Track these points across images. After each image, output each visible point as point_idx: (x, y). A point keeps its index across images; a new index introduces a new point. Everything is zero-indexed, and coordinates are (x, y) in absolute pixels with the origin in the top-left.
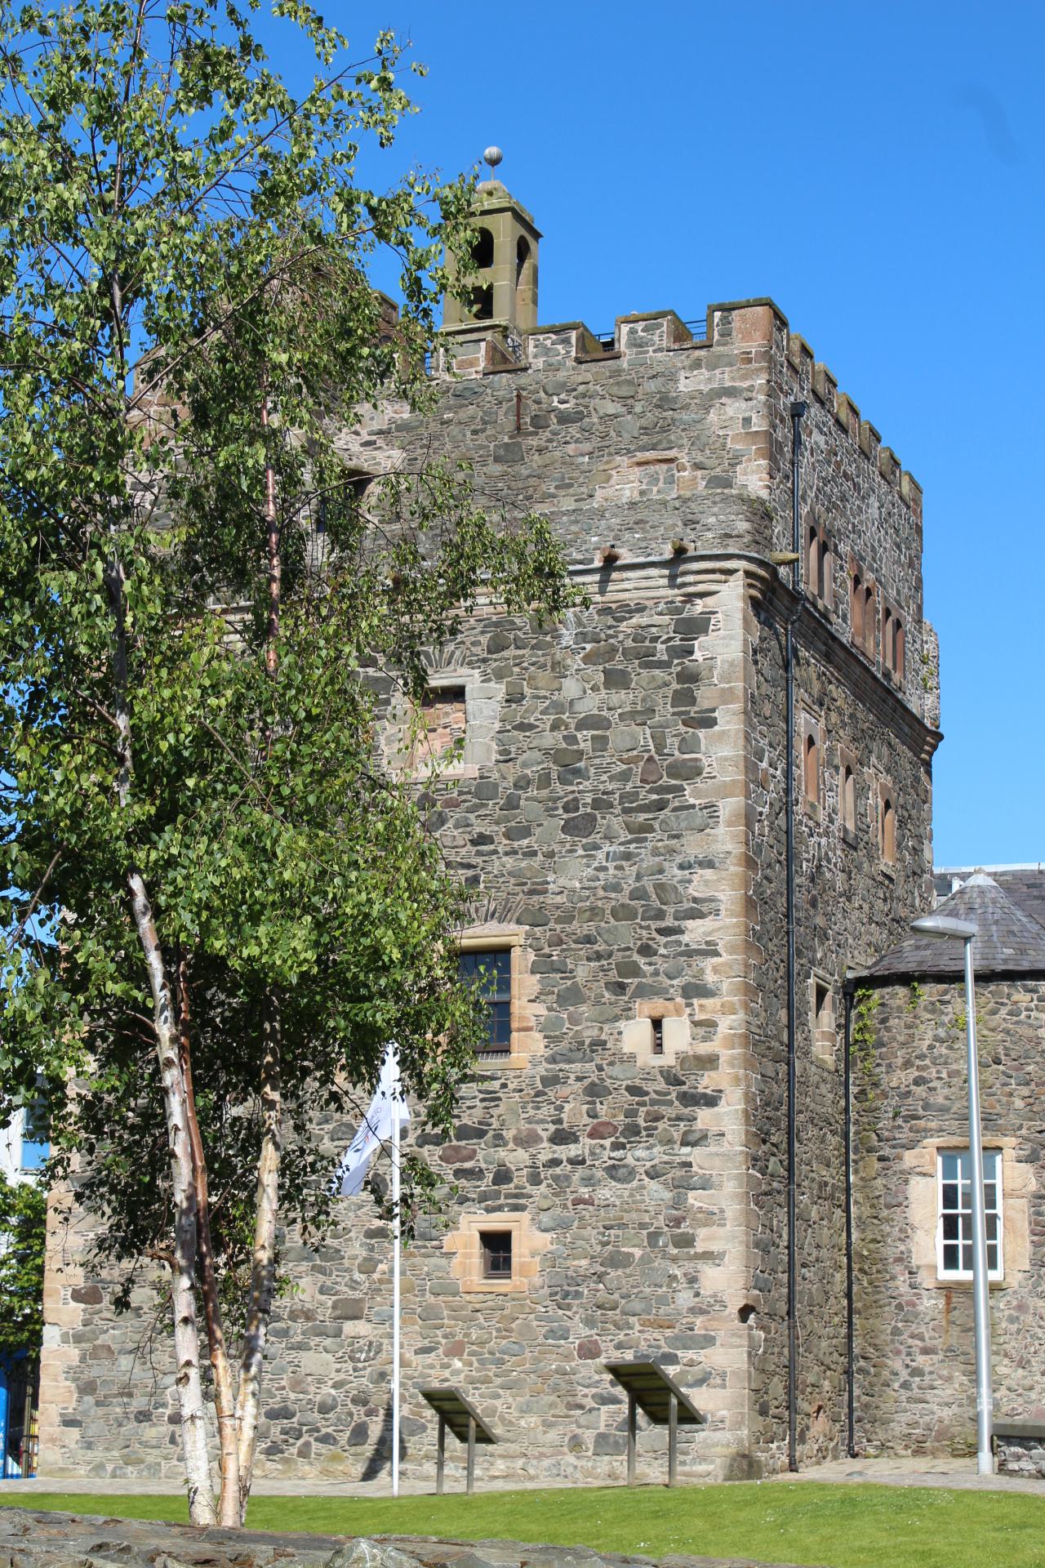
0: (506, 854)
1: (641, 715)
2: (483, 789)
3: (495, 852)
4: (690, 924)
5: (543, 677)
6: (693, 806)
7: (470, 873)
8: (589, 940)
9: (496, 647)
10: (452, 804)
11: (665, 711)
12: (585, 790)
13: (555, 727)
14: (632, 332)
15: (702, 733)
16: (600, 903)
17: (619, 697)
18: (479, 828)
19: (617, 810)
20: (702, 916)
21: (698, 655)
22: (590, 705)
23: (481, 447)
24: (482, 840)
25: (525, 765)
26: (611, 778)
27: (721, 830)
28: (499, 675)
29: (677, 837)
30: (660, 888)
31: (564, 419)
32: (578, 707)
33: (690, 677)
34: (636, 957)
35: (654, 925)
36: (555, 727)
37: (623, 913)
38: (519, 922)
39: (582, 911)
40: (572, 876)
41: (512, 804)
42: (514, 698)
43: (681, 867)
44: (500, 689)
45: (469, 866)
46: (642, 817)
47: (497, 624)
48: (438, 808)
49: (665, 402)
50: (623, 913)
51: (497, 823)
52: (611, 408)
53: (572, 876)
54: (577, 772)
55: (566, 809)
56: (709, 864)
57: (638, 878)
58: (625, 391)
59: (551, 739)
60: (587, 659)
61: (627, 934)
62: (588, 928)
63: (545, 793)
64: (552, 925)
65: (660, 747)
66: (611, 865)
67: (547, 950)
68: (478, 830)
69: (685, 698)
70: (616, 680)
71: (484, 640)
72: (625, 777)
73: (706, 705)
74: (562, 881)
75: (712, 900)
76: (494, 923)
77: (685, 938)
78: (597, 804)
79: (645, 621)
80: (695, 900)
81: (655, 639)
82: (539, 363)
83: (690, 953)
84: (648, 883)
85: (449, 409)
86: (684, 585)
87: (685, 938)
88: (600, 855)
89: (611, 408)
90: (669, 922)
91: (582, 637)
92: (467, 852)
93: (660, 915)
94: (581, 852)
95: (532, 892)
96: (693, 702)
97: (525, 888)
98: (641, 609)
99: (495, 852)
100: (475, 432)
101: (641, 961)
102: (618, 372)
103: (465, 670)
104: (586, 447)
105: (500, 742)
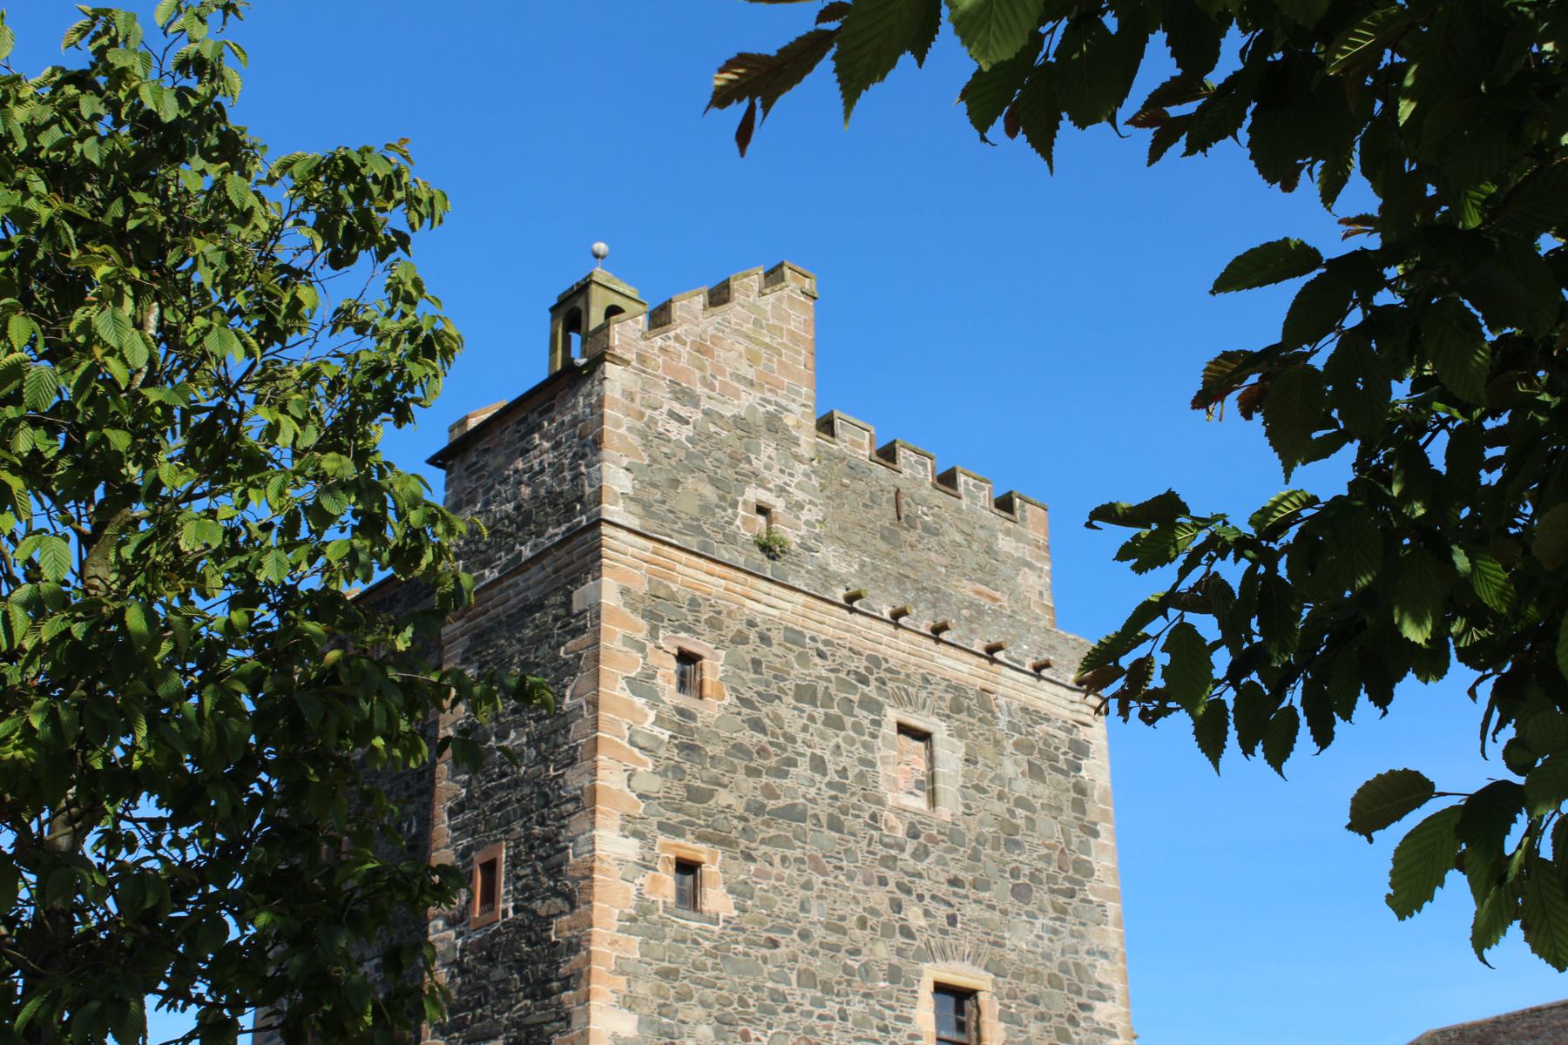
0: (975, 901)
1: (1055, 809)
2: (954, 836)
3: (966, 897)
4: (1098, 1004)
5: (989, 749)
6: (1091, 902)
7: (950, 911)
8: (1034, 1000)
9: (957, 708)
10: (931, 838)
11: (1068, 814)
12: (1026, 860)
13: (1001, 797)
14: (966, 483)
15: (1092, 840)
16: (1039, 968)
17: (1039, 788)
18: (955, 871)
19: (1045, 888)
20: (1104, 1000)
21: (1083, 773)
22: (1022, 787)
23: (871, 521)
24: (955, 882)
25: (981, 823)
26: (1040, 858)
27: (1110, 928)
28: (960, 734)
29: (1084, 924)
30: (1077, 965)
31: (926, 528)
32: (1016, 785)
33: (1080, 789)
34: (1066, 1025)
35: (1077, 999)
36: (1001, 797)
37: (1054, 981)
38: (986, 969)
39: (1029, 972)
40: (1022, 938)
41: (975, 857)
42: (969, 761)
43: (1089, 953)
44: (961, 747)
45: (951, 905)
46: (1061, 900)
47: (956, 688)
48: (922, 840)
49: (990, 551)
50: (1054, 981)
51: (966, 869)
52: (959, 538)
53: (1022, 938)
54: (1018, 844)
55: (1013, 876)
56: (1104, 955)
57: (1063, 952)
58: (968, 530)
59: (1000, 808)
60: (1017, 745)
61: (1061, 1002)
62: (1033, 989)
63: (996, 854)
64: (1008, 979)
65: (1068, 843)
66: (1046, 936)
67: (1006, 1001)
68: (953, 872)
69: (1079, 806)
70: (1035, 772)
71: (949, 697)
72: (1047, 859)
73: (1094, 819)
74: (1015, 941)
75: (1110, 988)
76: (967, 964)
77: (1096, 1016)
78: (1032, 876)
79: (1051, 731)
80: (1100, 985)
81: (1057, 749)
82: (907, 472)
83: (1101, 1031)
84: (1070, 959)
85: (847, 476)
86: (1078, 711)
87: (1096, 1016)
88: (1038, 923)
89: (959, 538)
90: (1084, 999)
91: (1013, 726)
92: (944, 890)
93: (1079, 992)
94: (1024, 918)
95: (995, 944)
96: (1084, 812)
97: (992, 938)
98: (1048, 720)
99: (966, 897)
100: (865, 505)
101: (1071, 1029)
102: (959, 510)
103: (935, 719)
104: (945, 560)
105: (964, 796)
